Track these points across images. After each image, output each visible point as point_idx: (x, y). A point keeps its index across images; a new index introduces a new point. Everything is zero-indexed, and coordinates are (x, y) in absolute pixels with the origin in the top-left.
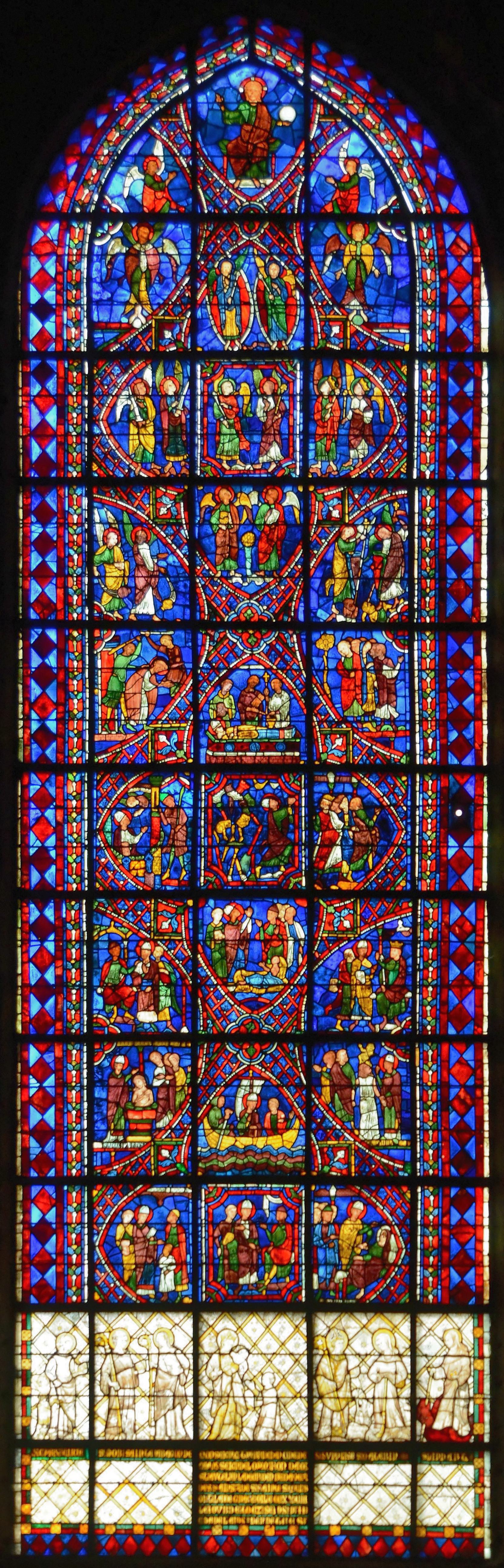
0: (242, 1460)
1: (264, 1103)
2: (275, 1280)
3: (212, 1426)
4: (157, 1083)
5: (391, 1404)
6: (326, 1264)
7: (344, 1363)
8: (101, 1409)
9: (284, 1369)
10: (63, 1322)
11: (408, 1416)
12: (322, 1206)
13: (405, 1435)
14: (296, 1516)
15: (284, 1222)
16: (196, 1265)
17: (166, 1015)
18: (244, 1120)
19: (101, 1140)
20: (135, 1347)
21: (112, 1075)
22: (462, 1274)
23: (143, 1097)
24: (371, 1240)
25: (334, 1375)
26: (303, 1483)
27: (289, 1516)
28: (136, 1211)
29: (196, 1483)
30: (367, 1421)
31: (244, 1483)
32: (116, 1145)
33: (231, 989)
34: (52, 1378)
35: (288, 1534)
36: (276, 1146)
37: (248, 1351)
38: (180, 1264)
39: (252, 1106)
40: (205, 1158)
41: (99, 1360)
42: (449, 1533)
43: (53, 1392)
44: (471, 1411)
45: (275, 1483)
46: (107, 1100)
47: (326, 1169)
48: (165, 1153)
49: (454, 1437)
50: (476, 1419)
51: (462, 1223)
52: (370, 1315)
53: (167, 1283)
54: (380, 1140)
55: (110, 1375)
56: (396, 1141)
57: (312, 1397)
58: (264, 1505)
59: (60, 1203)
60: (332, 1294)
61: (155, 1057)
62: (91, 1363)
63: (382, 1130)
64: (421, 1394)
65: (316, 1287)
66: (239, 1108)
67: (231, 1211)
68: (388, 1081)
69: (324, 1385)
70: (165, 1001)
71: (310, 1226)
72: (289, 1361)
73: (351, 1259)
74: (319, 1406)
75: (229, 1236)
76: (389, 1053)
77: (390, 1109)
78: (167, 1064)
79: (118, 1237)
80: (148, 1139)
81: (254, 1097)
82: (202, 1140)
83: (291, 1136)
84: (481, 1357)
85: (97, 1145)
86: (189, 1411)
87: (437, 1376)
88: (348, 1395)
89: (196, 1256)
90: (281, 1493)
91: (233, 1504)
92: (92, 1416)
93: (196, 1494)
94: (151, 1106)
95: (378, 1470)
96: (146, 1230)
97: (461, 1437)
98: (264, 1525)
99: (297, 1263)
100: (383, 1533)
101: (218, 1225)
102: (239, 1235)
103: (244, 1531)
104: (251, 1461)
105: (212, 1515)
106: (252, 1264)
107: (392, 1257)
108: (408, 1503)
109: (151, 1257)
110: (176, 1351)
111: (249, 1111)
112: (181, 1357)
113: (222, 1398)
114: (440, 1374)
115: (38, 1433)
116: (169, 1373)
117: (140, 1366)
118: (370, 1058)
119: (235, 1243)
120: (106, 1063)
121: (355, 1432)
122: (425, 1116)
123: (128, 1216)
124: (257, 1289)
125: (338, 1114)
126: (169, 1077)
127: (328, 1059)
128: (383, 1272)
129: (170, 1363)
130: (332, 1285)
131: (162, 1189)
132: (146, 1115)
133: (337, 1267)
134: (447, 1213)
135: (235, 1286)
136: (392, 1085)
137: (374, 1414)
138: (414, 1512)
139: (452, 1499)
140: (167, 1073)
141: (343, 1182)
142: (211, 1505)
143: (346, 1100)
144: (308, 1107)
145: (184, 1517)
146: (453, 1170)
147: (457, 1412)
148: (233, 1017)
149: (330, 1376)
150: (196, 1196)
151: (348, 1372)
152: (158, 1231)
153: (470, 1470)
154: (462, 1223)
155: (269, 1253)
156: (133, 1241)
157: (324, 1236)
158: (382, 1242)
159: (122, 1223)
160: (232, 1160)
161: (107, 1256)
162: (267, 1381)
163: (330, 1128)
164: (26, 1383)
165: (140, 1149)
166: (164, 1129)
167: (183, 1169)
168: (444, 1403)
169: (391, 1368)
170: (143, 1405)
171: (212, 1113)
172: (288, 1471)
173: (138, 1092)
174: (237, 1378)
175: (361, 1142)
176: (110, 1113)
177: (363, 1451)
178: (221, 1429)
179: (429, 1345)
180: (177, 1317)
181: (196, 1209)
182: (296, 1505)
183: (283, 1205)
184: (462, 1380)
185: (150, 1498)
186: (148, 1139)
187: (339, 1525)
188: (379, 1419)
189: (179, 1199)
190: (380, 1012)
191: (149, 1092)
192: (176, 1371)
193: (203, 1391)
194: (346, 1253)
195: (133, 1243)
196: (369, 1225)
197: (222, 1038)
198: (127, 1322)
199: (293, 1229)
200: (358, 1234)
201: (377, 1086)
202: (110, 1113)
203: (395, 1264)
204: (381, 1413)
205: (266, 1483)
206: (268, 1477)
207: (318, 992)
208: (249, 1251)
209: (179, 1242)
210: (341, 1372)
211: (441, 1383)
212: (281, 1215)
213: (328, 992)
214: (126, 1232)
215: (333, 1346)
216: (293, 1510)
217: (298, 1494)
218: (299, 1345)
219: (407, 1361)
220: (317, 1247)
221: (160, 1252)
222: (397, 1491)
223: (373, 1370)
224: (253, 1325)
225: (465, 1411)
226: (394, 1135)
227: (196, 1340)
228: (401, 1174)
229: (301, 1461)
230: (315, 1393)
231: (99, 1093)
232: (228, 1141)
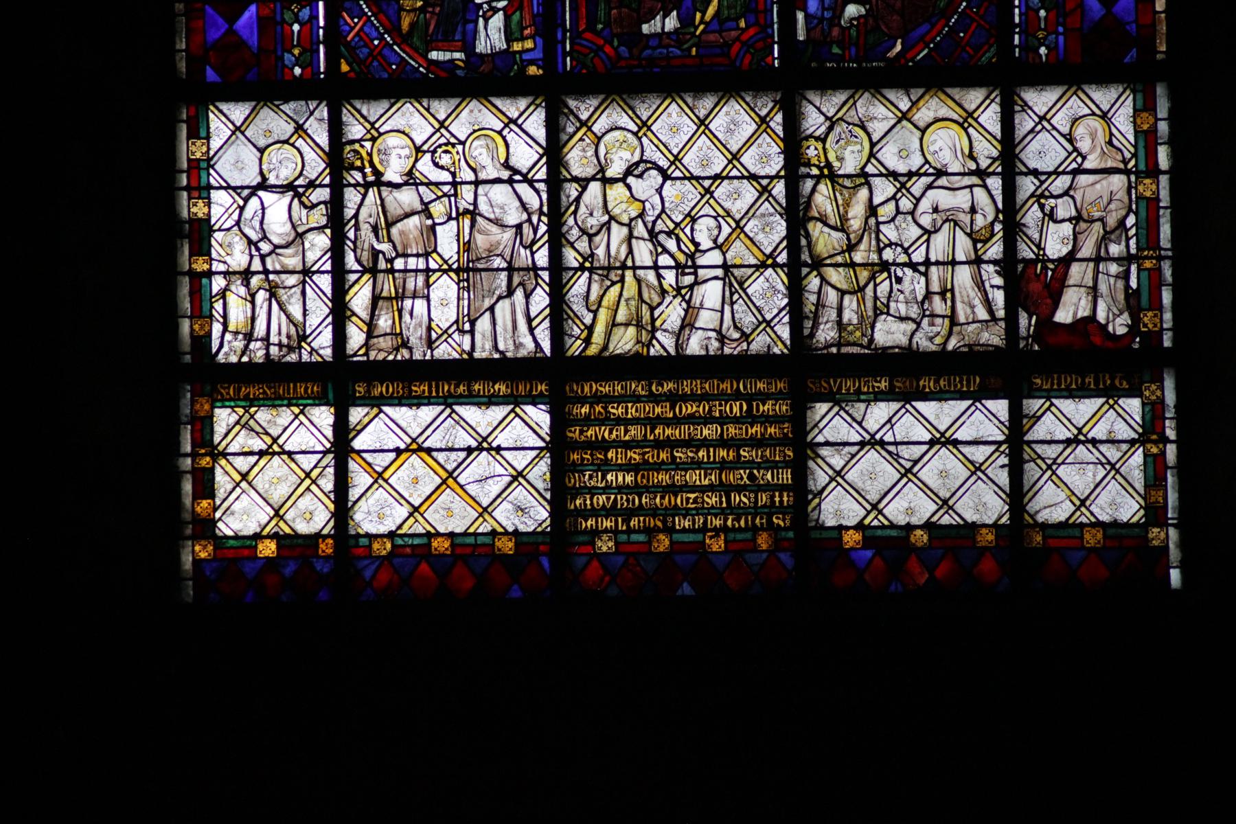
0: (655, 399)
2: (716, 26)
3: (590, 329)
5: (964, 275)
7: (863, 193)
8: (360, 299)
9: (738, 207)
11: (999, 297)
13: (994, 337)
14: (771, 510)
25: (844, 219)
26: (783, 441)
27: (755, 510)
29: (558, 447)
30: (914, 312)
31: (659, 444)
34: (254, 236)
35: (755, 549)
41: (352, 197)
42: (1092, 538)
44: (1134, 283)
45: (723, 443)
49: (1097, 340)
52: (916, 93)
53: (491, 35)
55: (375, 229)
57: (798, 262)
58: (703, 489)
60: (836, 50)
64: (1026, 252)
69: (825, 240)
72: (749, 193)
74: (814, 282)
84: (1153, 171)
86: (540, 300)
87: (1061, 213)
88: (874, 257)
90: (737, 463)
91: (637, 489)
92: (340, 313)
95: (942, 413)
97: (1114, 337)
98: (704, 529)
100: (951, 540)
103: (663, 543)
104: (674, 399)
105: (594, 512)
108: (1003, 478)
112: (523, 189)
117: (438, 209)
121: (889, 333)
130: (836, 32)
137: (928, 295)
138: (1017, 495)
139: (1096, 465)
142: (593, 491)
147: (1103, 287)
151: (872, 210)
153: (1133, 405)
162: (704, 232)
168: (1076, 270)
169: (961, 200)
172: (750, 418)
174: (640, 230)
177: (908, 374)
178: (608, 335)
179: (1042, 152)
182: (768, 487)
184: (1112, 221)
185: (465, 477)
187: (860, 526)
188: (938, 306)
204: (942, 294)
205: (705, 443)
210: (857, 212)
211: (1067, 228)
215: (841, 159)
216: (764, 498)
217: (772, 465)
218: (767, 157)
219: (995, 183)
222: (979, 454)
223: (925, 205)
224: (673, 121)
225: (1120, 284)
227: (554, 152)
229: (777, 396)
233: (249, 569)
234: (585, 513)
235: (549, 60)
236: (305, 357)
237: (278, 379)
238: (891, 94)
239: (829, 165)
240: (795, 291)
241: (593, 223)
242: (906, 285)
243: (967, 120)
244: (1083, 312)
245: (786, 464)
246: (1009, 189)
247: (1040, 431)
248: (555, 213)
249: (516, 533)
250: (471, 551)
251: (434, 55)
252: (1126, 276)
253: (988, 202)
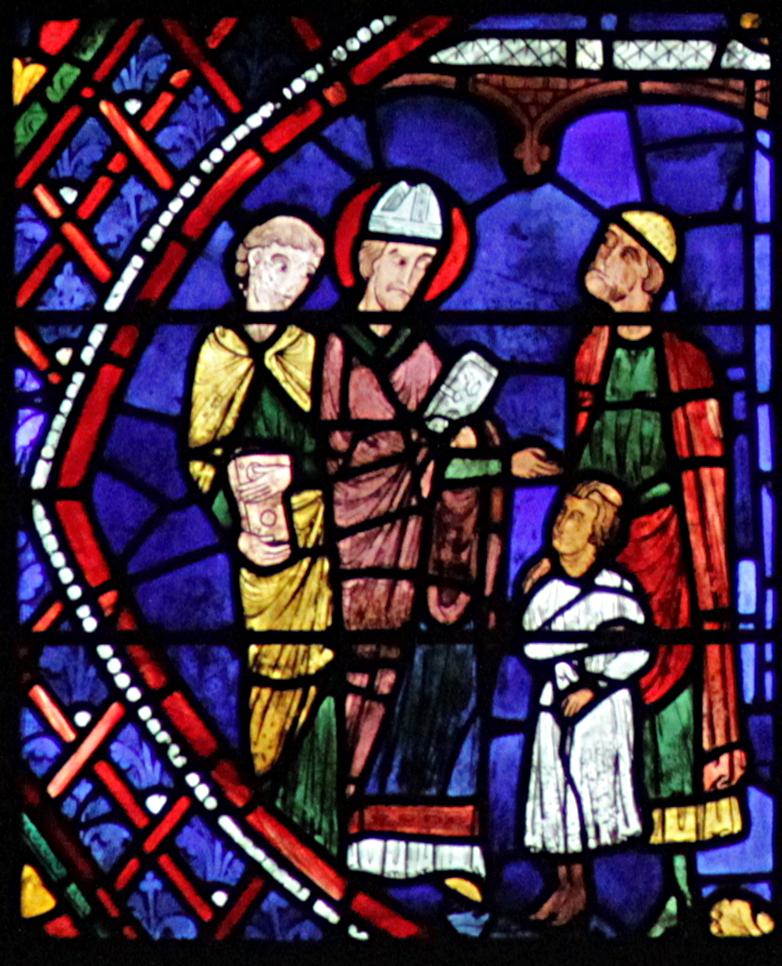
28: (343, 227)
38: (678, 638)
79: (201, 428)
96: (421, 364)
109: (454, 580)
152: (509, 372)
156: (317, 451)
159: (236, 315)
189: (674, 120)
195: (316, 471)
209: (675, 464)
214: (262, 381)
221: (524, 544)
251: (368, 855)
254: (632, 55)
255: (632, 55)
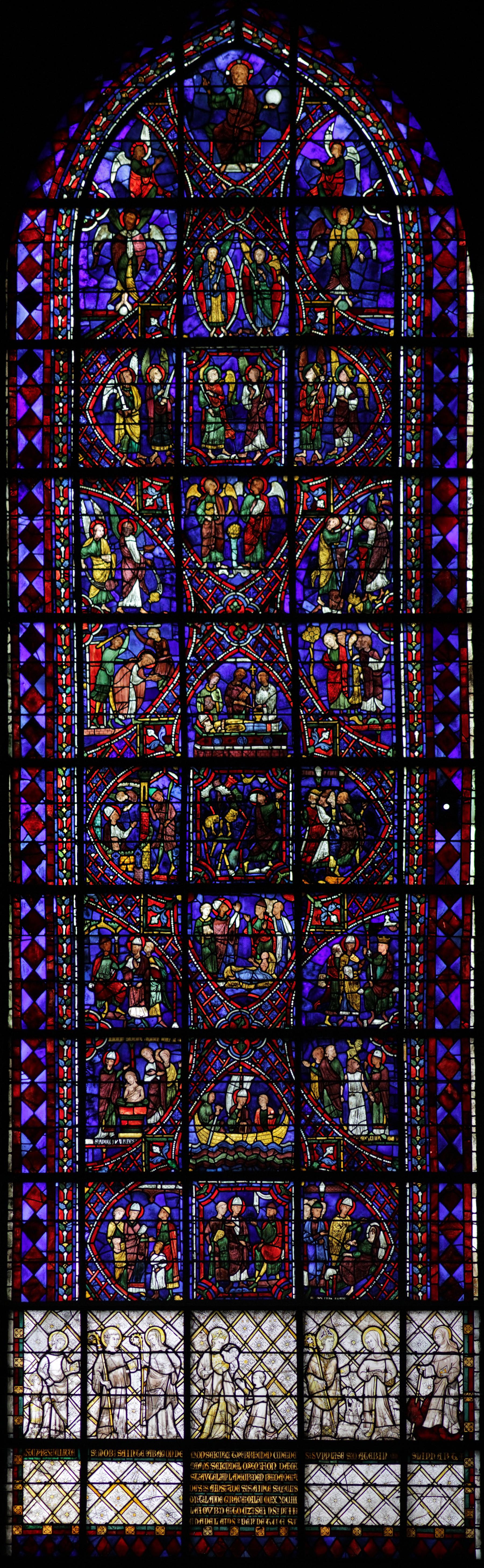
0: (233, 1460)
1: (254, 1099)
2: (265, 1278)
3: (203, 1425)
4: (148, 1079)
5: (381, 1403)
6: (316, 1261)
7: (334, 1362)
8: (94, 1409)
9: (274, 1367)
10: (55, 1321)
11: (397, 1414)
12: (312, 1202)
13: (394, 1434)
14: (287, 1516)
15: (274, 1218)
16: (187, 1262)
17: (157, 1010)
18: (234, 1116)
19: (92, 1137)
20: (126, 1344)
21: (104, 1070)
22: (451, 1271)
23: (134, 1093)
24: (360, 1237)
25: (324, 1374)
26: (293, 1483)
27: (279, 1516)
28: (127, 1209)
29: (186, 1483)
30: (357, 1420)
31: (234, 1483)
32: (107, 1142)
33: (221, 984)
34: (44, 1377)
36: (266, 1142)
37: (239, 1349)
38: (170, 1262)
39: (242, 1101)
40: (195, 1154)
41: (91, 1358)
43: (45, 1391)
44: (461, 1409)
45: (265, 1483)
46: (98, 1096)
47: (316, 1165)
48: (156, 1149)
49: (443, 1436)
50: (466, 1417)
51: (451, 1218)
52: (360, 1313)
53: (158, 1281)
54: (368, 1135)
55: (102, 1374)
56: (384, 1137)
57: (302, 1395)
58: (255, 1506)
59: (52, 1201)
60: (322, 1291)
61: (146, 1053)
62: (83, 1362)
63: (371, 1126)
64: (410, 1392)
65: (306, 1283)
66: (229, 1104)
67: (222, 1208)
68: (376, 1077)
69: (315, 1384)
70: (156, 996)
71: (299, 1221)
72: (279, 1360)
73: (341, 1256)
74: (309, 1405)
75: (220, 1233)
76: (377, 1048)
77: (378, 1104)
78: (157, 1060)
79: (109, 1234)
80: (139, 1135)
81: (243, 1093)
82: (192, 1137)
83: (280, 1131)
85: (89, 1142)
86: (180, 1411)
87: (427, 1374)
88: (338, 1393)
89: (187, 1253)
90: (272, 1493)
91: (223, 1505)
92: (84, 1415)
93: (186, 1496)
94: (142, 1102)
95: (368, 1470)
96: (137, 1227)
97: (451, 1435)
98: (255, 1525)
99: (287, 1260)
101: (209, 1221)
102: (229, 1232)
103: (235, 1531)
104: (242, 1461)
105: (203, 1516)
106: (243, 1261)
107: (381, 1253)
109: (142, 1254)
110: (168, 1350)
111: (239, 1107)
112: (173, 1356)
113: (214, 1397)
114: (429, 1372)
115: (31, 1433)
116: (160, 1372)
117: (132, 1365)
118: (358, 1053)
119: (225, 1240)
120: (98, 1059)
121: (345, 1431)
122: (413, 1110)
123: (119, 1214)
124: (248, 1286)
125: (327, 1109)
126: (159, 1073)
127: (317, 1055)
128: (373, 1269)
129: (161, 1361)
130: (322, 1282)
131: (154, 1186)
132: (137, 1111)
133: (327, 1264)
134: (434, 1209)
135: (227, 1283)
136: (380, 1080)
137: (364, 1412)
140: (158, 1069)
141: (331, 1178)
142: (202, 1505)
143: (334, 1095)
144: (298, 1102)
145: (177, 1517)
146: (440, 1165)
147: (447, 1410)
148: (224, 1012)
149: (319, 1374)
150: (187, 1193)
151: (338, 1370)
152: (149, 1228)
154: (451, 1218)
155: (260, 1251)
157: (314, 1232)
158: (372, 1239)
159: (113, 1220)
160: (223, 1156)
161: (99, 1253)
162: (258, 1380)
163: (319, 1124)
164: (19, 1382)
165: (131, 1145)
166: (155, 1125)
167: (174, 1166)
168: (434, 1402)
169: (380, 1366)
170: (134, 1404)
171: (203, 1109)
172: (278, 1471)
173: (130, 1088)
174: (228, 1377)
175: (350, 1138)
176: (101, 1109)
178: (211, 1428)
179: (419, 1343)
180: (168, 1316)
181: (187, 1206)
183: (272, 1201)
184: (451, 1378)
185: (141, 1497)
186: (139, 1135)
188: (368, 1418)
189: (170, 1195)
190: (369, 1007)
191: (140, 1088)
192: (168, 1370)
193: (195, 1390)
194: (336, 1249)
196: (358, 1221)
197: (213, 1033)
198: (120, 1321)
199: (284, 1226)
200: (347, 1231)
201: (366, 1081)
202: (101, 1109)
203: (384, 1260)
204: (370, 1412)
205: (256, 1483)
206: (258, 1477)
207: (307, 988)
208: (240, 1248)
209: (170, 1239)
210: (331, 1370)
211: (430, 1381)
212: (271, 1212)
213: (317, 987)
214: (117, 1229)
215: (323, 1345)
216: (283, 1510)
217: (288, 1494)
219: (397, 1358)
220: (308, 1243)
223: (363, 1368)
224: (244, 1324)
225: (455, 1409)
226: (382, 1131)
227: (187, 1339)
228: (389, 1169)
229: (291, 1461)
230: (306, 1392)
231: (91, 1089)
232: (218, 1138)
233: (39, 1540)
234: (198, 1516)
235: (185, 1293)
236: (67, 1437)
237: (54, 1447)
238: (348, 1313)
239: (318, 1347)
240: (301, 1409)
241: (205, 1373)
242: (353, 1407)
243: (384, 1327)
244: (437, 1422)
245: (295, 1494)
246: (403, 1361)
247: (415, 1481)
248: (187, 1368)
249: (166, 1525)
250: (144, 1533)
251: (131, 1290)
252: (458, 1405)
253: (392, 1367)
254: (164, 1187)
255: (164, 1187)
